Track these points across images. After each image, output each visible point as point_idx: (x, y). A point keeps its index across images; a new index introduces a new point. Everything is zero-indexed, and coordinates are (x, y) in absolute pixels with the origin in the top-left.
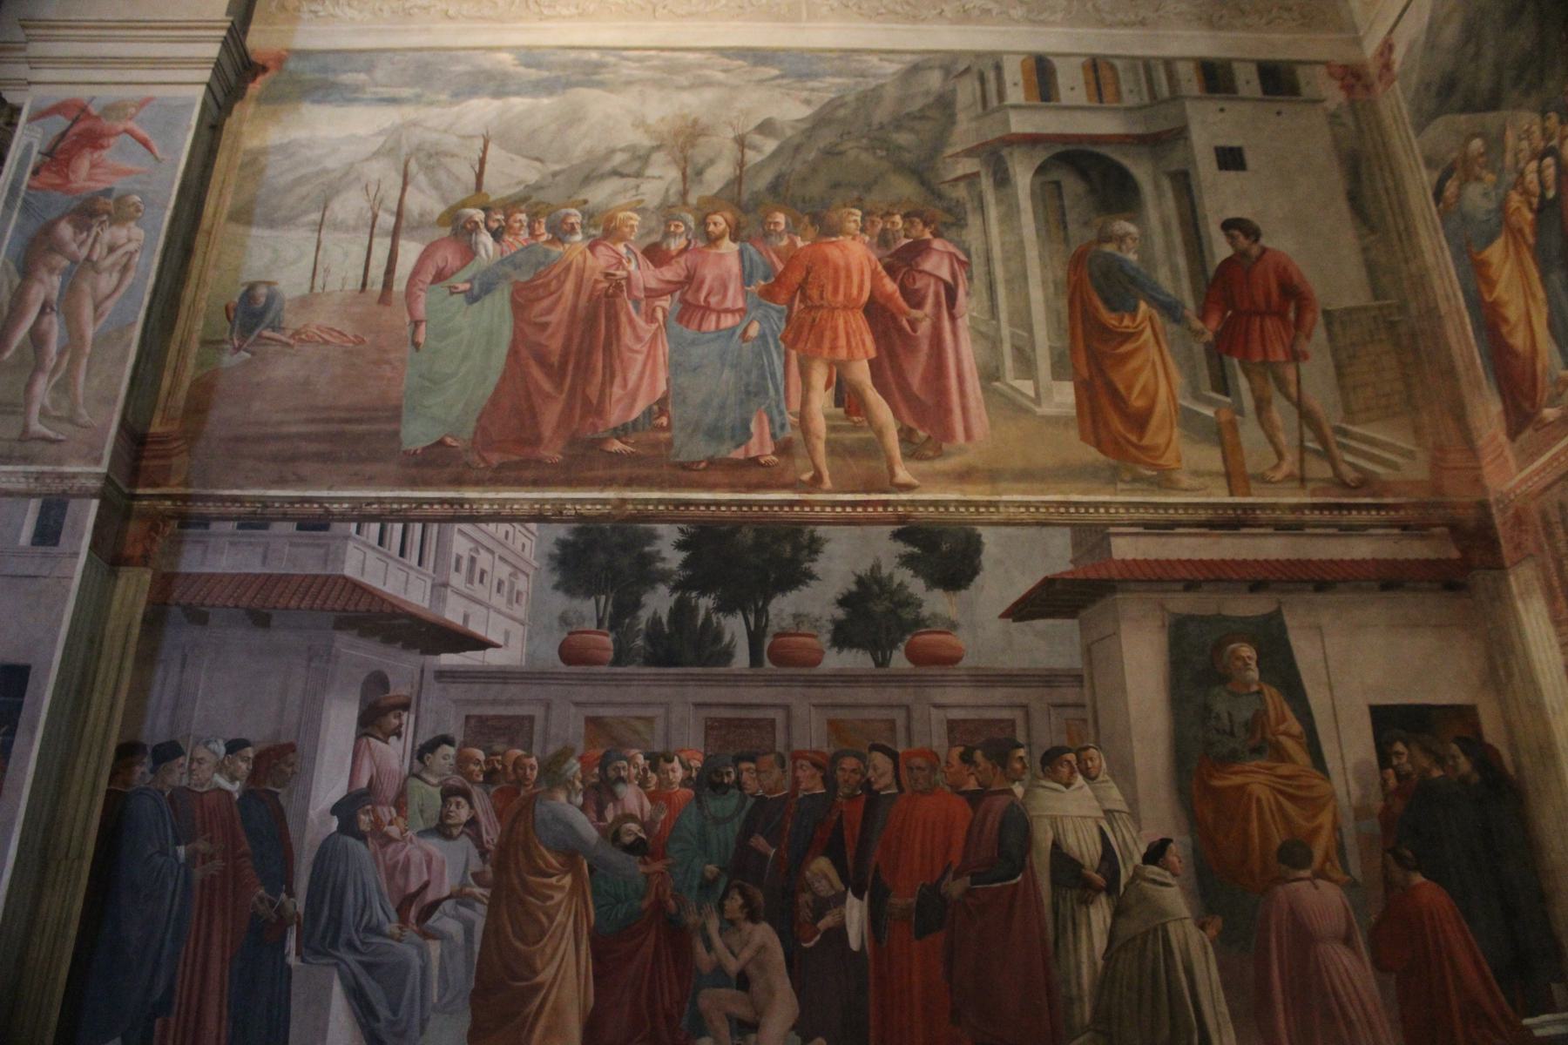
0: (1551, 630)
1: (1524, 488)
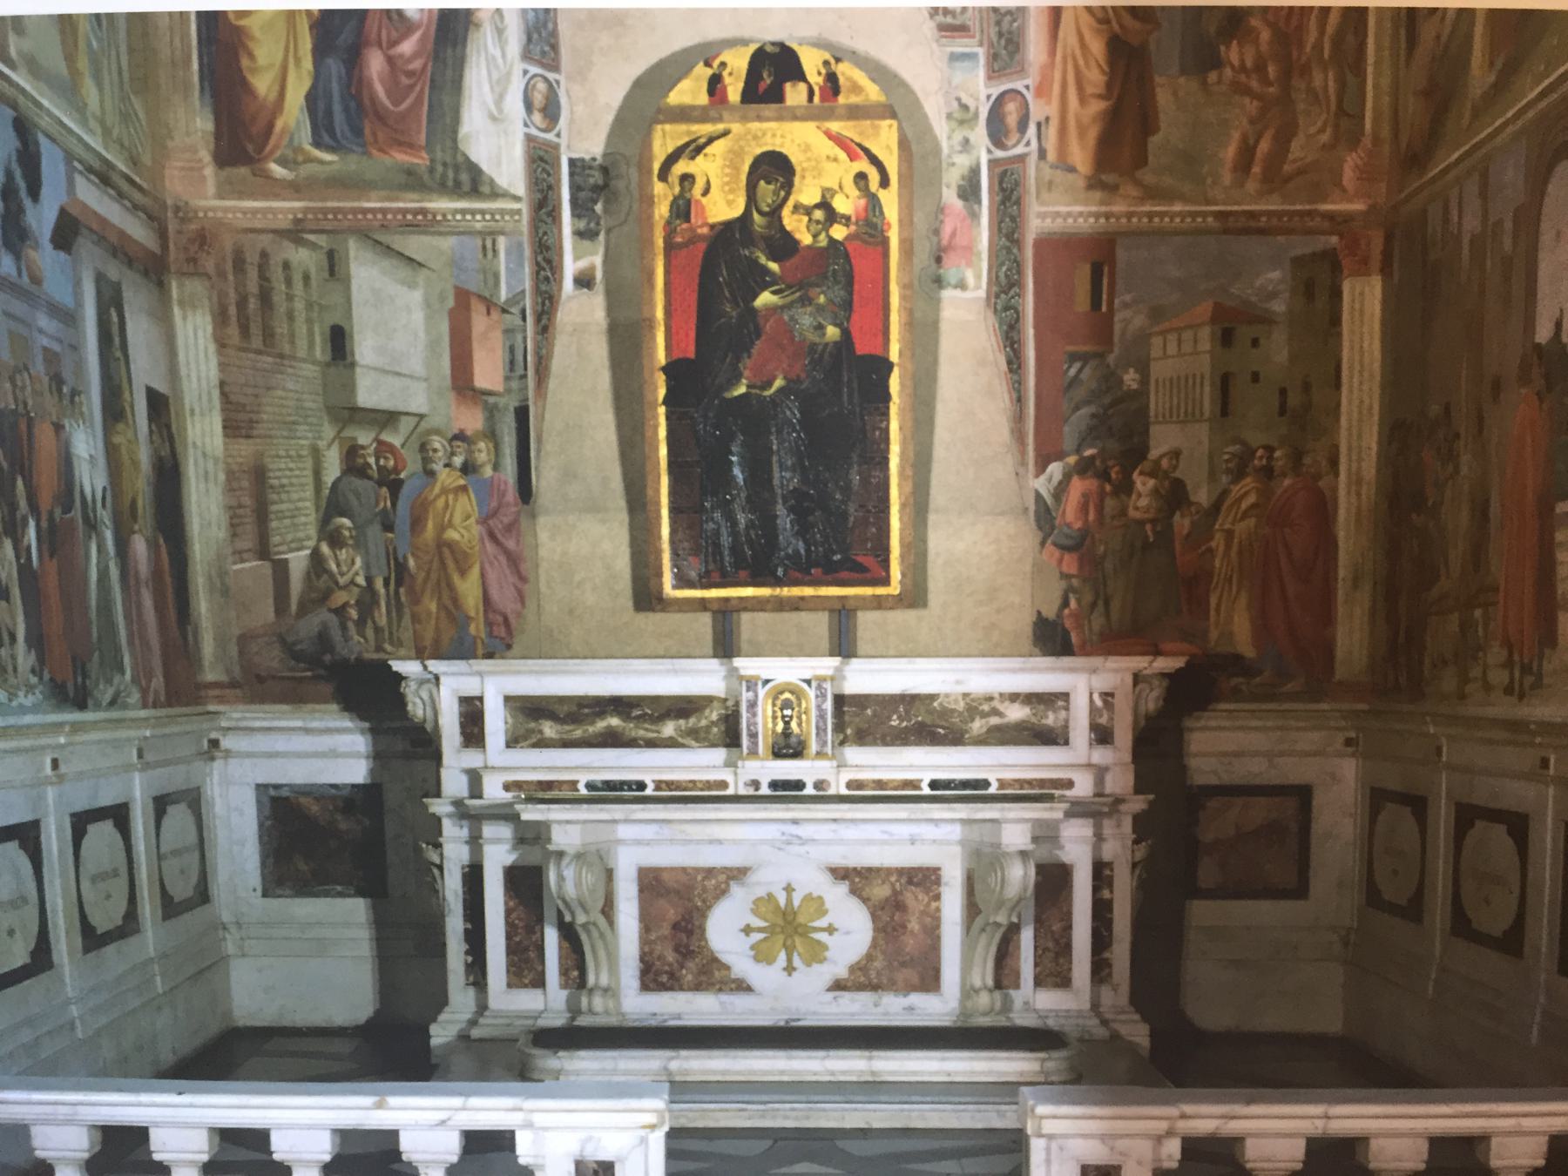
0: (212, 348)
1: (220, 214)
